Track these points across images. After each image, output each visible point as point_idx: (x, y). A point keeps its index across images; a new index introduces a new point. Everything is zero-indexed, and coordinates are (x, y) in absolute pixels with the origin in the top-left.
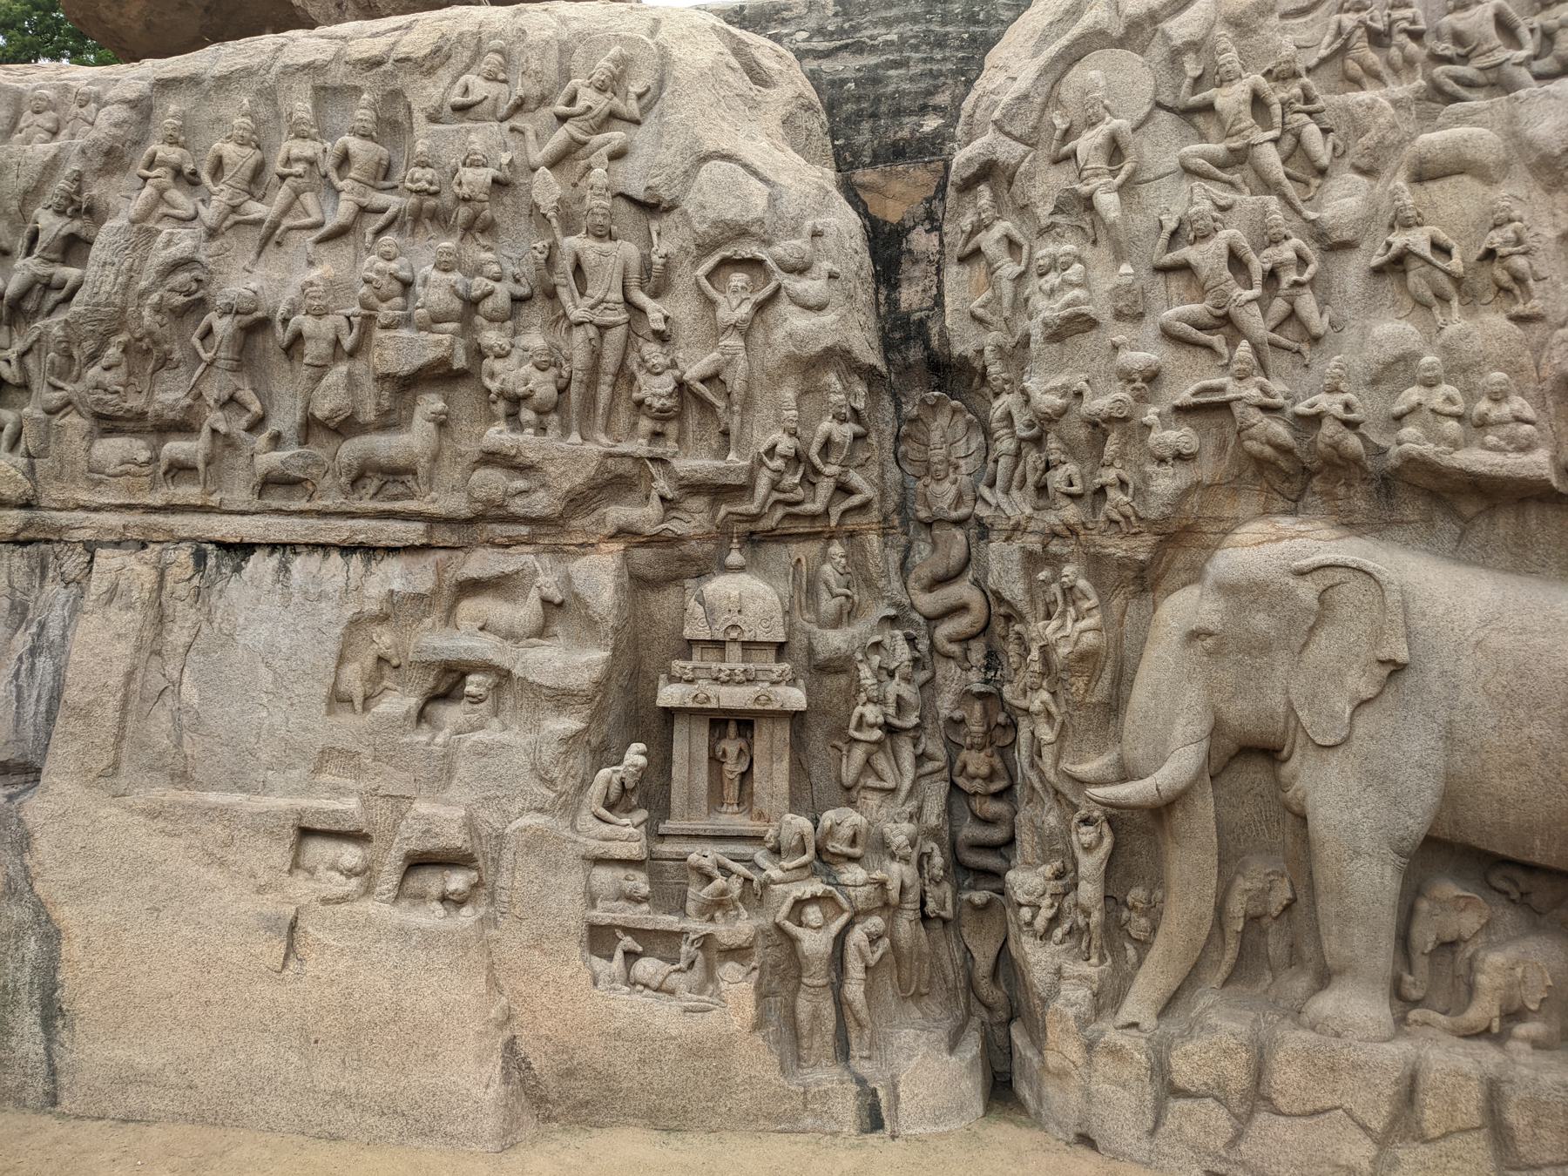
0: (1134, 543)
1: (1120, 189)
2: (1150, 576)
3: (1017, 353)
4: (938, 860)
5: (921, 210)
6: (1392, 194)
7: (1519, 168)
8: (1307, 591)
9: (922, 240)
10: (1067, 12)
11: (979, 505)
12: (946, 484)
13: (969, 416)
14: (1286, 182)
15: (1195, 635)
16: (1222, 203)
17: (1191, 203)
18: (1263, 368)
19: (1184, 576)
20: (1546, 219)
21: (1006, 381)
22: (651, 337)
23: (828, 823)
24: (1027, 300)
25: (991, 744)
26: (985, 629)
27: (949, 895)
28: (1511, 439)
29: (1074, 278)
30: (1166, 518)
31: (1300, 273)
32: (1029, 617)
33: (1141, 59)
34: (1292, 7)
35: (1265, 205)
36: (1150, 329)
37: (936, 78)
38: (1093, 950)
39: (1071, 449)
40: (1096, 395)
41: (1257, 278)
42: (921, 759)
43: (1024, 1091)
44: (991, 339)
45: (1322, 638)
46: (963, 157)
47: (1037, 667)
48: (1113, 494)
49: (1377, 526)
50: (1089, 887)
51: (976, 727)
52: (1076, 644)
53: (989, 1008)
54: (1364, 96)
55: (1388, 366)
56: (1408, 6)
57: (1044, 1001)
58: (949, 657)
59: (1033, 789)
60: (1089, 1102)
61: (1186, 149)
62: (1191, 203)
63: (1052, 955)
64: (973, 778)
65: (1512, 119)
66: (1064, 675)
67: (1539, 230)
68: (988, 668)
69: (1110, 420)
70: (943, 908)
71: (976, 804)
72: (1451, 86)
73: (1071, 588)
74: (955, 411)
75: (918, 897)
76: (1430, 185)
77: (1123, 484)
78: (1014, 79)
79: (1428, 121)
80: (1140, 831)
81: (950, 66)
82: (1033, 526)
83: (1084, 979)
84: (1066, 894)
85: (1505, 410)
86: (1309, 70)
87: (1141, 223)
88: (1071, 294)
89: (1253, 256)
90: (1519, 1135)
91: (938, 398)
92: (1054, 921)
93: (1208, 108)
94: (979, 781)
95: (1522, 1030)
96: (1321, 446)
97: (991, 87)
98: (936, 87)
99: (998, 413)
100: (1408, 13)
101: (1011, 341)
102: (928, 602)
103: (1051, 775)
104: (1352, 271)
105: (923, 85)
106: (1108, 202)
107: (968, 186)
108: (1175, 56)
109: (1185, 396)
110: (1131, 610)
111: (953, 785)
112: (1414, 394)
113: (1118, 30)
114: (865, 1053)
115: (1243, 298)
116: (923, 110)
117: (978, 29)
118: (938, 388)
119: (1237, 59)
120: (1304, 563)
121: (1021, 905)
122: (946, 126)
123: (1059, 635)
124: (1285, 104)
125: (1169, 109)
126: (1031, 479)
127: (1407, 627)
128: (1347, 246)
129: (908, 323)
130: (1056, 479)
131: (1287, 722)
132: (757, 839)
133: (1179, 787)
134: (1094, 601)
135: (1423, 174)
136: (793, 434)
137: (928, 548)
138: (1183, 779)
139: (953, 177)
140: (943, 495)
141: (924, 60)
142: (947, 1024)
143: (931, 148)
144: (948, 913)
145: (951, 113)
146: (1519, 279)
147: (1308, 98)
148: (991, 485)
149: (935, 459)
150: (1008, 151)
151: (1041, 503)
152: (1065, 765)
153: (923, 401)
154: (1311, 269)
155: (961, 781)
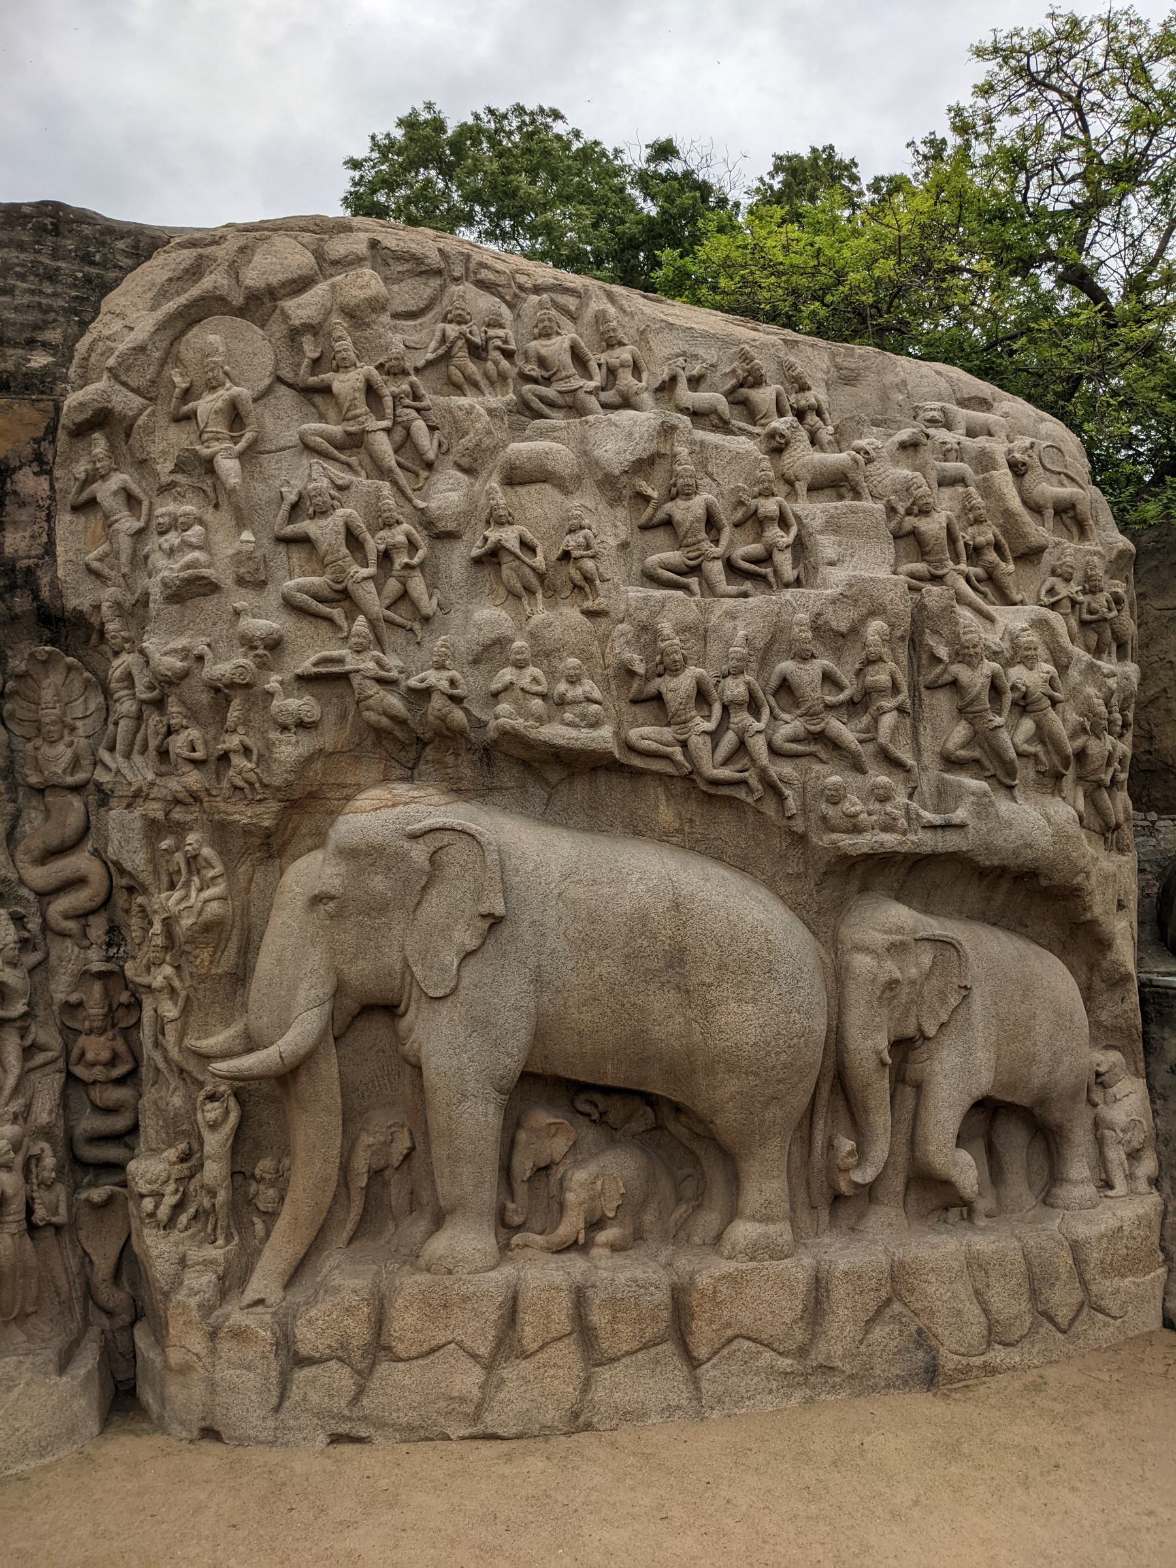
0: (259, 809)
1: (241, 456)
2: (275, 842)
3: (136, 612)
4: (49, 1161)
5: (27, 451)
6: (488, 493)
7: (588, 482)
8: (419, 853)
9: (28, 482)
10: (186, 271)
11: (99, 768)
12: (61, 747)
13: (87, 674)
14: (397, 470)
15: (318, 900)
16: (340, 482)
17: (310, 479)
18: (379, 643)
19: (309, 842)
20: (610, 530)
21: (126, 640)
24: (146, 557)
25: (113, 1026)
26: (107, 902)
27: (63, 1198)
28: (583, 717)
29: (194, 540)
30: (290, 785)
31: (412, 558)
32: (152, 889)
33: (261, 332)
34: (402, 309)
35: (378, 489)
36: (272, 597)
37: (46, 312)
38: (219, 1231)
39: (193, 714)
40: (218, 659)
41: (373, 557)
43: (148, 1396)
44: (108, 594)
45: (433, 897)
46: (76, 399)
47: (159, 941)
48: (238, 761)
49: (479, 791)
50: (215, 1166)
51: (95, 1010)
52: (200, 914)
53: (110, 1314)
54: (464, 401)
55: (486, 648)
56: (501, 326)
57: (166, 1295)
58: (63, 935)
59: (157, 1070)
60: (214, 1392)
61: (305, 426)
62: (310, 479)
63: (176, 1244)
64: (93, 1065)
65: (583, 440)
66: (187, 948)
67: (602, 537)
68: (110, 945)
70: (56, 1212)
71: (96, 1094)
72: (537, 404)
73: (195, 857)
74: (70, 669)
75: (23, 1207)
76: (518, 489)
77: (247, 751)
78: (131, 329)
79: (518, 432)
80: (265, 1101)
81: (62, 303)
82: (155, 792)
83: (208, 1263)
84: (192, 1176)
85: (578, 691)
86: (417, 370)
87: (261, 492)
89: (368, 536)
90: (601, 1333)
91: (50, 653)
92: (178, 1208)
94: (98, 1067)
95: (602, 1237)
96: (431, 718)
97: (106, 332)
98: (46, 322)
99: (118, 672)
100: (501, 332)
101: (130, 599)
102: (39, 876)
103: (174, 1053)
104: (456, 559)
105: (31, 317)
106: (229, 467)
107: (81, 431)
108: (295, 334)
109: (306, 666)
110: (258, 877)
111: (70, 1077)
112: (507, 674)
113: (238, 299)
115: (360, 575)
116: (31, 343)
117: (93, 271)
118: (52, 642)
119: (351, 347)
121: (142, 1196)
122: (56, 364)
123: (183, 905)
124: (394, 397)
125: (290, 386)
126: (153, 743)
127: (503, 882)
128: (452, 536)
129: (13, 570)
130: (178, 744)
131: (403, 978)
133: (302, 1052)
134: (219, 869)
135: (514, 478)
137: (41, 817)
138: (309, 1042)
139: (63, 420)
140: (57, 758)
141: (32, 292)
142: (59, 1342)
143: (41, 386)
144: (61, 1218)
145: (64, 351)
146: (588, 579)
147: (416, 397)
148: (112, 749)
149: (48, 720)
150: (125, 401)
151: (164, 768)
152: (190, 1042)
153: (32, 655)
154: (421, 553)
155: (79, 1071)
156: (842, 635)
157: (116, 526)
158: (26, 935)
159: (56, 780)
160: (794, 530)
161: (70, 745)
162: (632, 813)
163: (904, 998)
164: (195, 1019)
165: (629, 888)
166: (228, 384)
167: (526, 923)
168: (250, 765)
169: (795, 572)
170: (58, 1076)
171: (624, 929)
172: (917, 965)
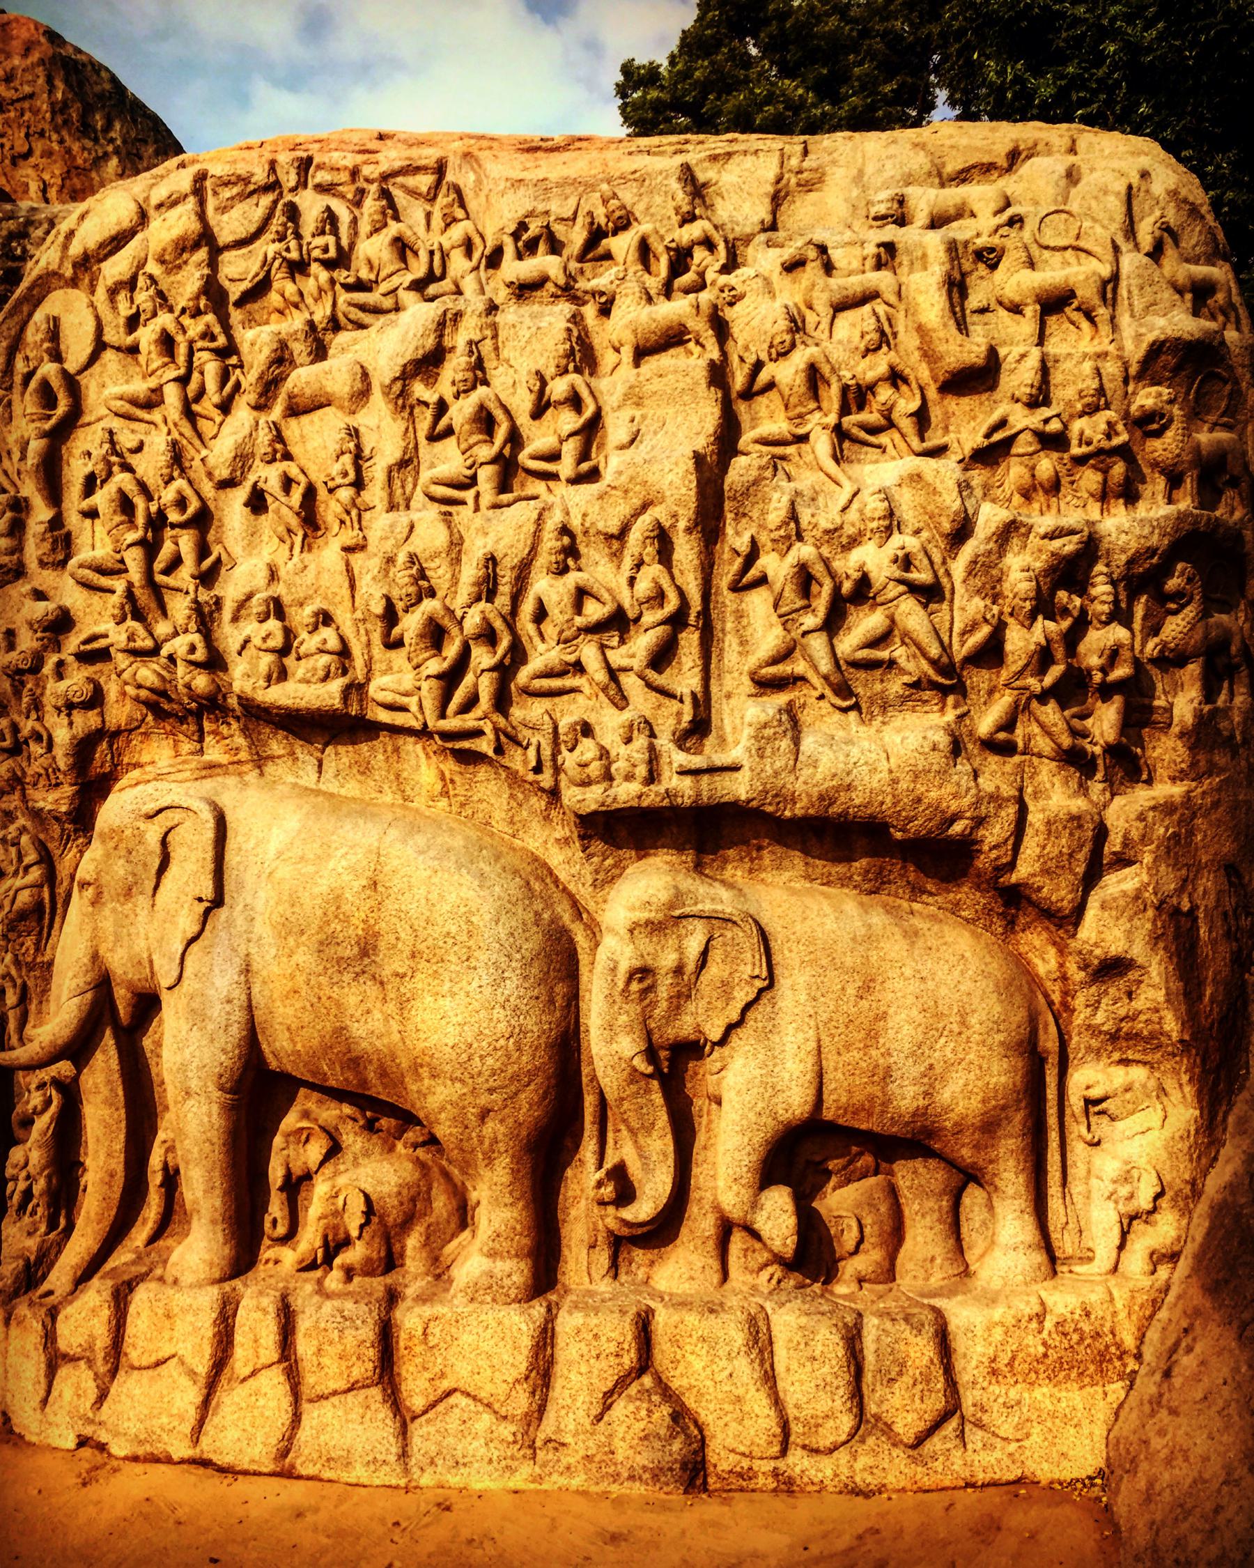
15: (84, 885)
30: (72, 767)
69: (20, 672)
76: (305, 419)
77: (38, 737)
120: (151, 807)
134: (31, 857)
156: (612, 536)
160: (589, 411)
162: (398, 776)
163: (664, 990)
164: (33, 1007)
165: (331, 865)
167: (240, 907)
168: (41, 751)
169: (585, 466)
171: (319, 913)
172: (680, 949)
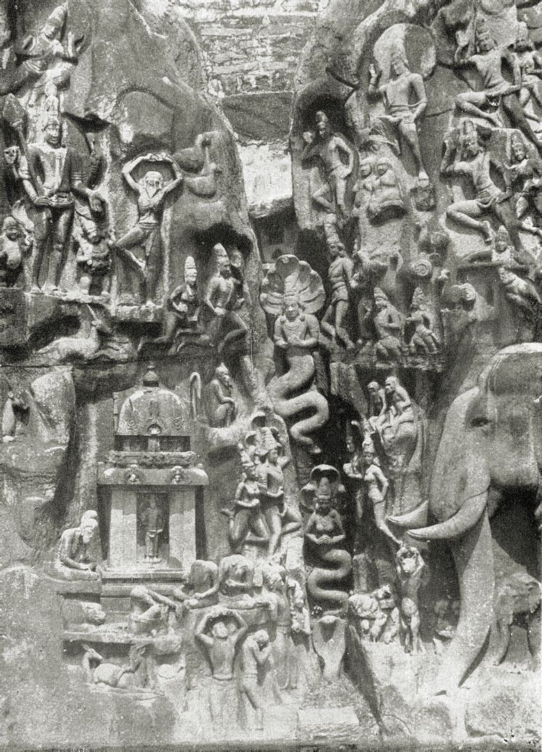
4: (300, 593)
12: (298, 320)
21: (340, 249)
22: (90, 216)
23: (226, 567)
42: (286, 520)
73: (394, 392)
88: (387, 192)
91: (290, 259)
92: (383, 628)
93: (472, 66)
99: (336, 272)
114: (259, 727)
130: (381, 318)
132: (176, 580)
134: (408, 401)
136: (194, 287)
144: (307, 630)
155: (312, 537)
157: (334, 172)
158: (279, 444)
159: (295, 343)
161: (303, 320)
166: (408, 72)
170: (300, 539)
